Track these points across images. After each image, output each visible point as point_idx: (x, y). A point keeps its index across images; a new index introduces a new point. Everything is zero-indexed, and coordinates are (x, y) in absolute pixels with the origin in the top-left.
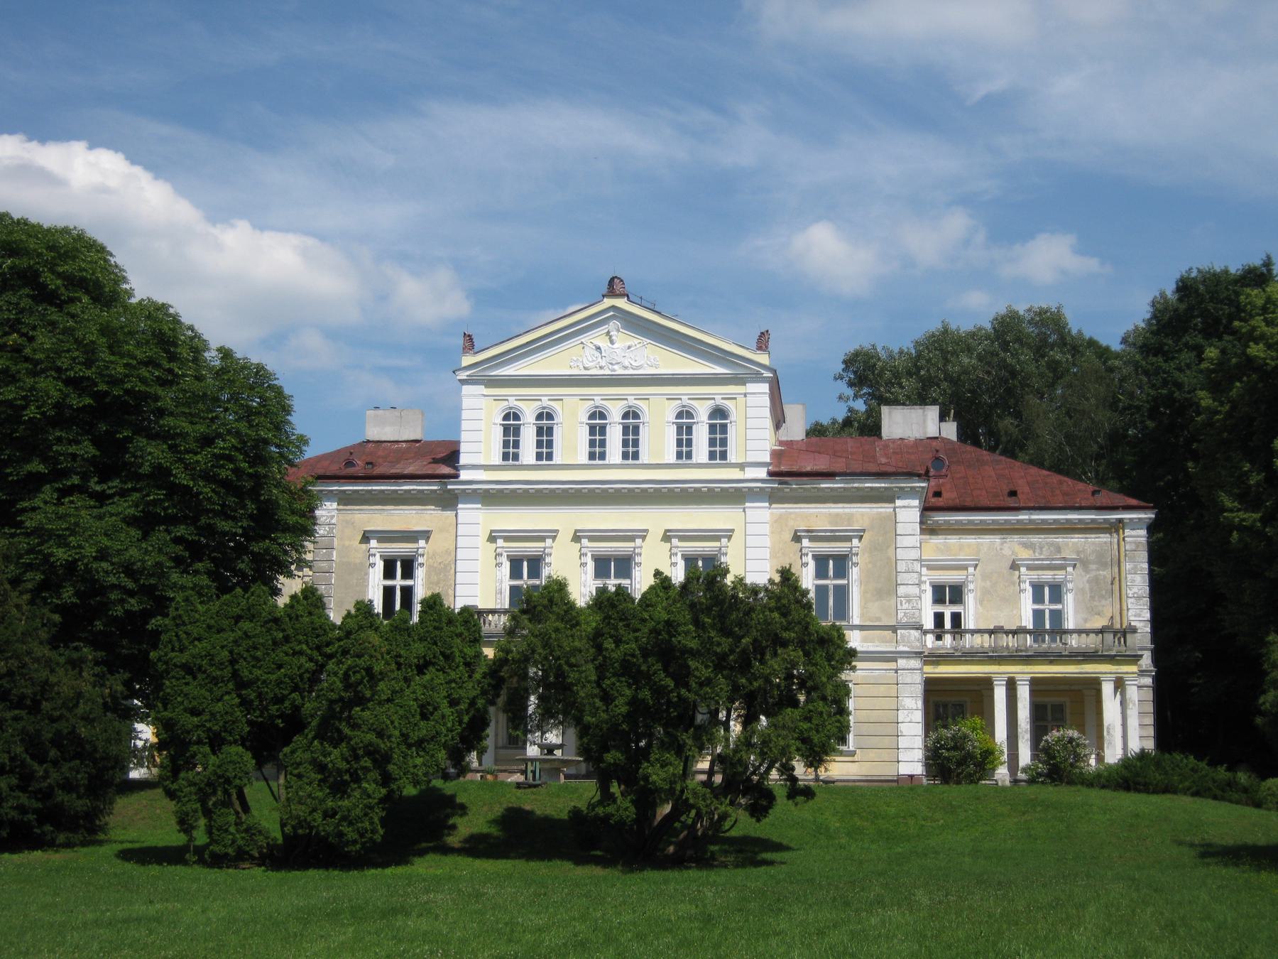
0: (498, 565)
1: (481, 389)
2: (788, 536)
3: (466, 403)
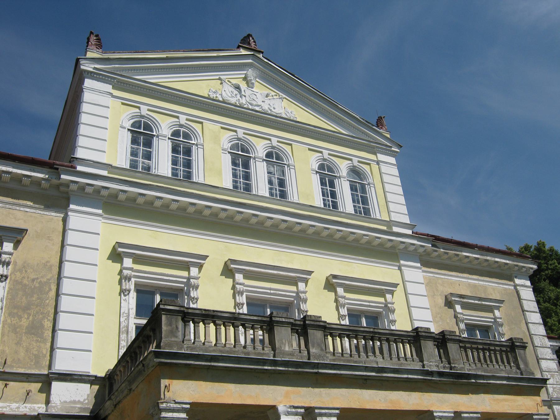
0: (123, 292)
1: (108, 88)
2: (441, 301)
3: (87, 96)
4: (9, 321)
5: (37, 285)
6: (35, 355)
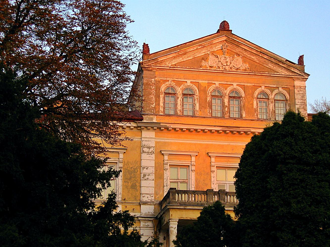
4: (125, 184)
5: (133, 170)
6: (134, 196)
